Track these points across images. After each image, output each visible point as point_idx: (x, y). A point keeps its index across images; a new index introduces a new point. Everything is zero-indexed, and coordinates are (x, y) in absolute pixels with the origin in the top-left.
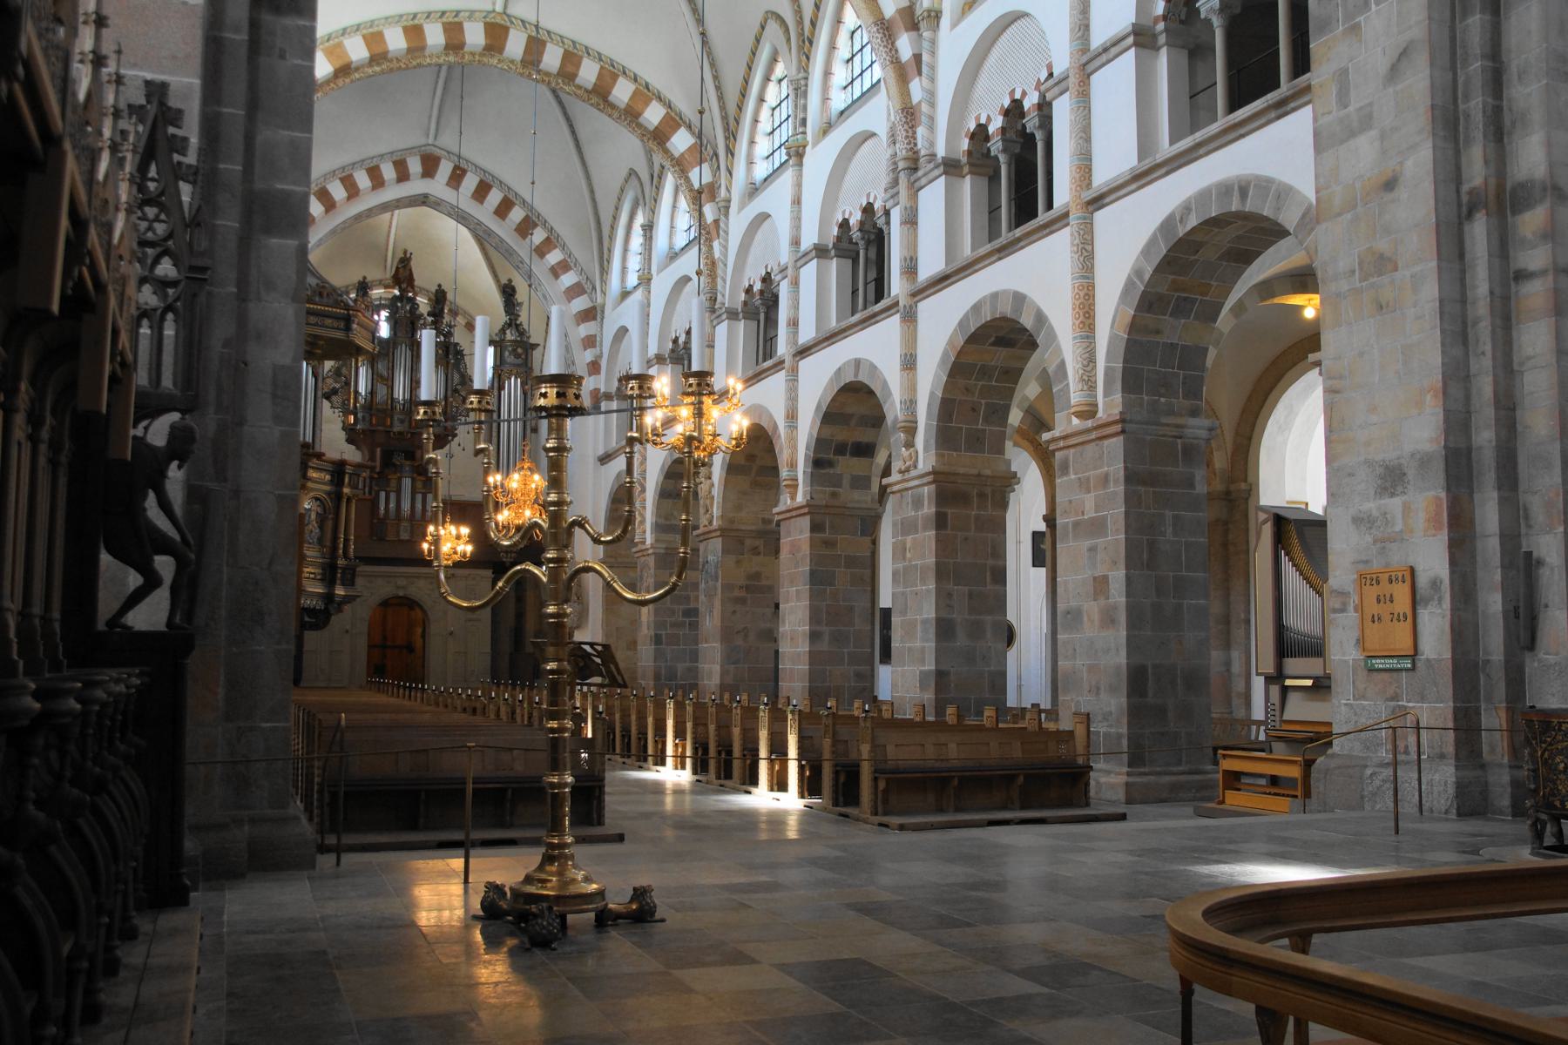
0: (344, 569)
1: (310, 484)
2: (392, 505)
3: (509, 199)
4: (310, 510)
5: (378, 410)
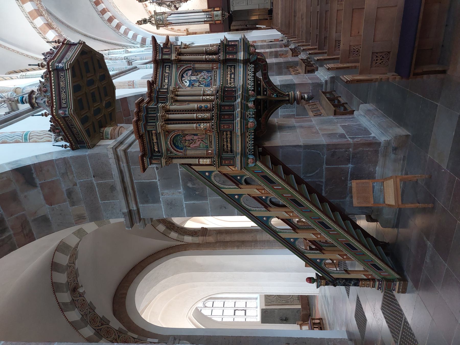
0: (226, 53)
1: (171, 88)
4: (190, 81)
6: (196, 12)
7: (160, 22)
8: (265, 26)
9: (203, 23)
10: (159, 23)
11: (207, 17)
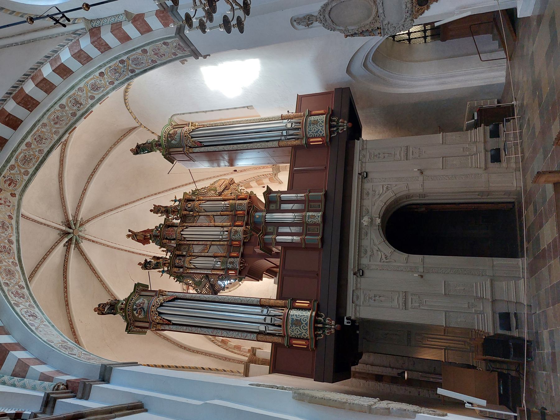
6: (239, 302)
7: (140, 314)
8: (484, 402)
9: (254, 336)
10: (137, 315)
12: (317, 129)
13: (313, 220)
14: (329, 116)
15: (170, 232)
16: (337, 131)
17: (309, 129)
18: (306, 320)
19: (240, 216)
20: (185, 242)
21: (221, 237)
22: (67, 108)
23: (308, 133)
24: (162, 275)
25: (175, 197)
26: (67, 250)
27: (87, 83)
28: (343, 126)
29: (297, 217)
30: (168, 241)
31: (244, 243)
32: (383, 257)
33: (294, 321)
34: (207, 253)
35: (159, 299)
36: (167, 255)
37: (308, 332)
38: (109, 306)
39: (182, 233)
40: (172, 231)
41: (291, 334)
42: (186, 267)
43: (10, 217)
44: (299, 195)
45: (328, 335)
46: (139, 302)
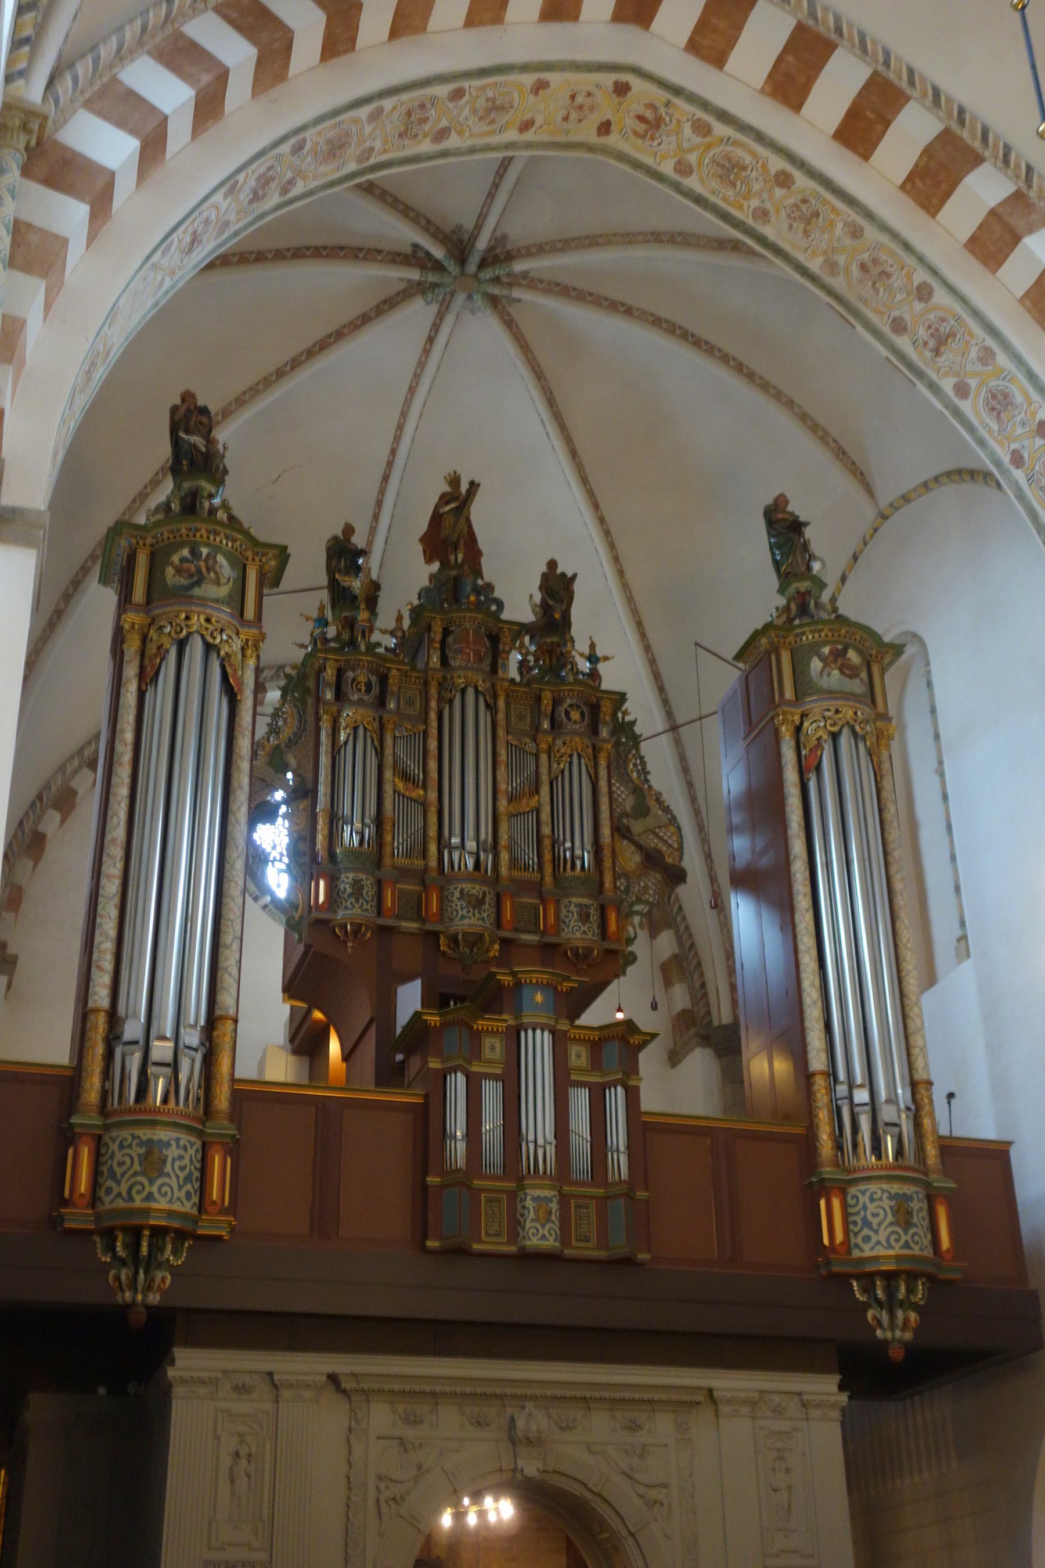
2: (491, 1122)
3: (888, 83)
5: (404, 873)
7: (178, 571)
10: (176, 559)
11: (162, 1050)
12: (879, 1224)
13: (532, 1215)
14: (931, 1270)
15: (471, 646)
16: (872, 1302)
17: (876, 1193)
18: (166, 1194)
19: (537, 916)
20: (433, 704)
21: (455, 840)
22: (919, 306)
23: (862, 1188)
24: (308, 619)
25: (606, 658)
26: (399, 255)
27: (1012, 379)
28: (892, 1326)
29: (540, 1152)
30: (439, 637)
31: (436, 935)
32: (396, 1490)
33: (161, 1152)
34: (394, 792)
35: (230, 637)
36: (384, 632)
37: (121, 1204)
38: (204, 449)
39: (470, 693)
40: (477, 653)
41: (113, 1140)
42: (339, 712)
43: (526, 126)
44: (623, 1159)
45: (111, 1280)
46: (221, 566)
